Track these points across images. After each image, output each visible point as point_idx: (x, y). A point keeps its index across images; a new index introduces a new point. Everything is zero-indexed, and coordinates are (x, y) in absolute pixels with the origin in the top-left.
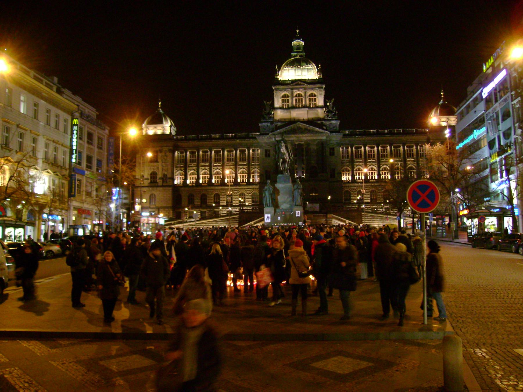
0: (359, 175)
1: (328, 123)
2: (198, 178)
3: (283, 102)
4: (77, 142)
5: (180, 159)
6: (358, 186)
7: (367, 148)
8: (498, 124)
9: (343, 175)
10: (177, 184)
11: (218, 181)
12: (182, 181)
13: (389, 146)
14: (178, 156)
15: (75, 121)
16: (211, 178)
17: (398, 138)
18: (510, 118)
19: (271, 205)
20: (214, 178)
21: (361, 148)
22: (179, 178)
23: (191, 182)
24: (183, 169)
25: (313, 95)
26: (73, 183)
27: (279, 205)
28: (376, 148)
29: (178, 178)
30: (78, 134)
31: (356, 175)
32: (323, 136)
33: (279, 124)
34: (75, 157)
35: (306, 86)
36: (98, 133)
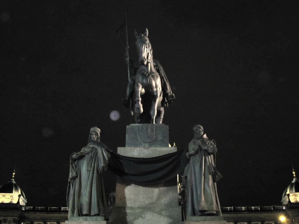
17: (256, 215)
19: (95, 210)
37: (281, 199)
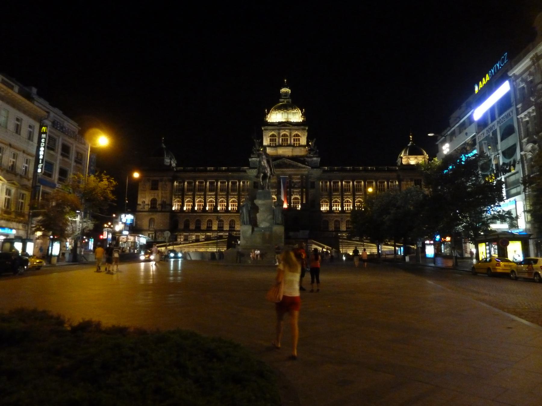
0: (336, 206)
1: (309, 160)
2: (194, 206)
3: (270, 141)
4: (44, 151)
5: (178, 188)
6: (335, 216)
7: (344, 183)
8: (497, 143)
9: (322, 206)
10: (175, 210)
11: (211, 208)
12: (179, 207)
13: (363, 181)
14: (177, 185)
15: (44, 129)
16: (205, 206)
18: (513, 136)
19: (248, 223)
20: (208, 206)
21: (338, 182)
22: (177, 205)
23: (188, 208)
24: (180, 196)
25: (297, 135)
26: (37, 195)
27: (258, 223)
28: (351, 183)
29: (176, 204)
30: (47, 142)
31: (334, 206)
32: (305, 171)
34: (41, 167)
35: (291, 127)
36: (76, 147)
37: (397, 160)
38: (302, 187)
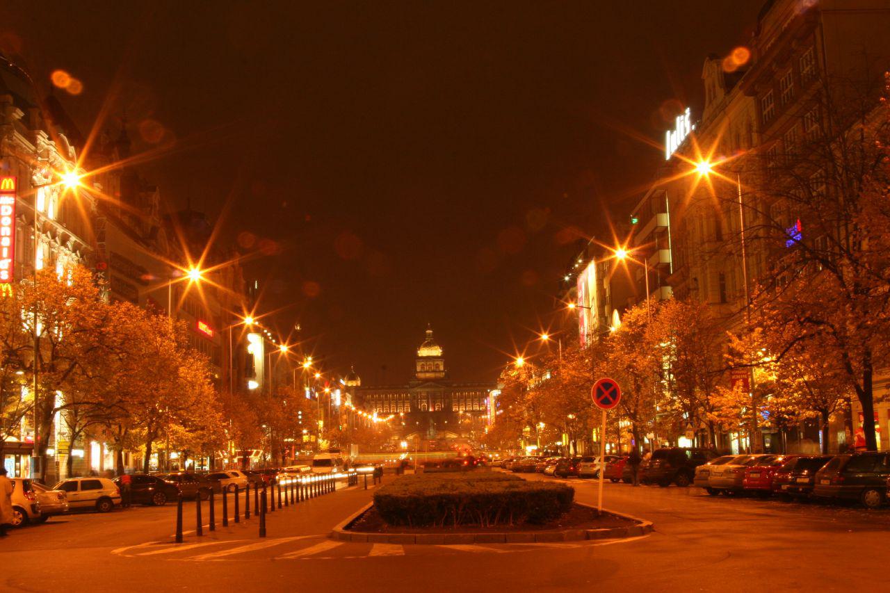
25: (437, 364)
33: (420, 382)
38: (441, 398)
